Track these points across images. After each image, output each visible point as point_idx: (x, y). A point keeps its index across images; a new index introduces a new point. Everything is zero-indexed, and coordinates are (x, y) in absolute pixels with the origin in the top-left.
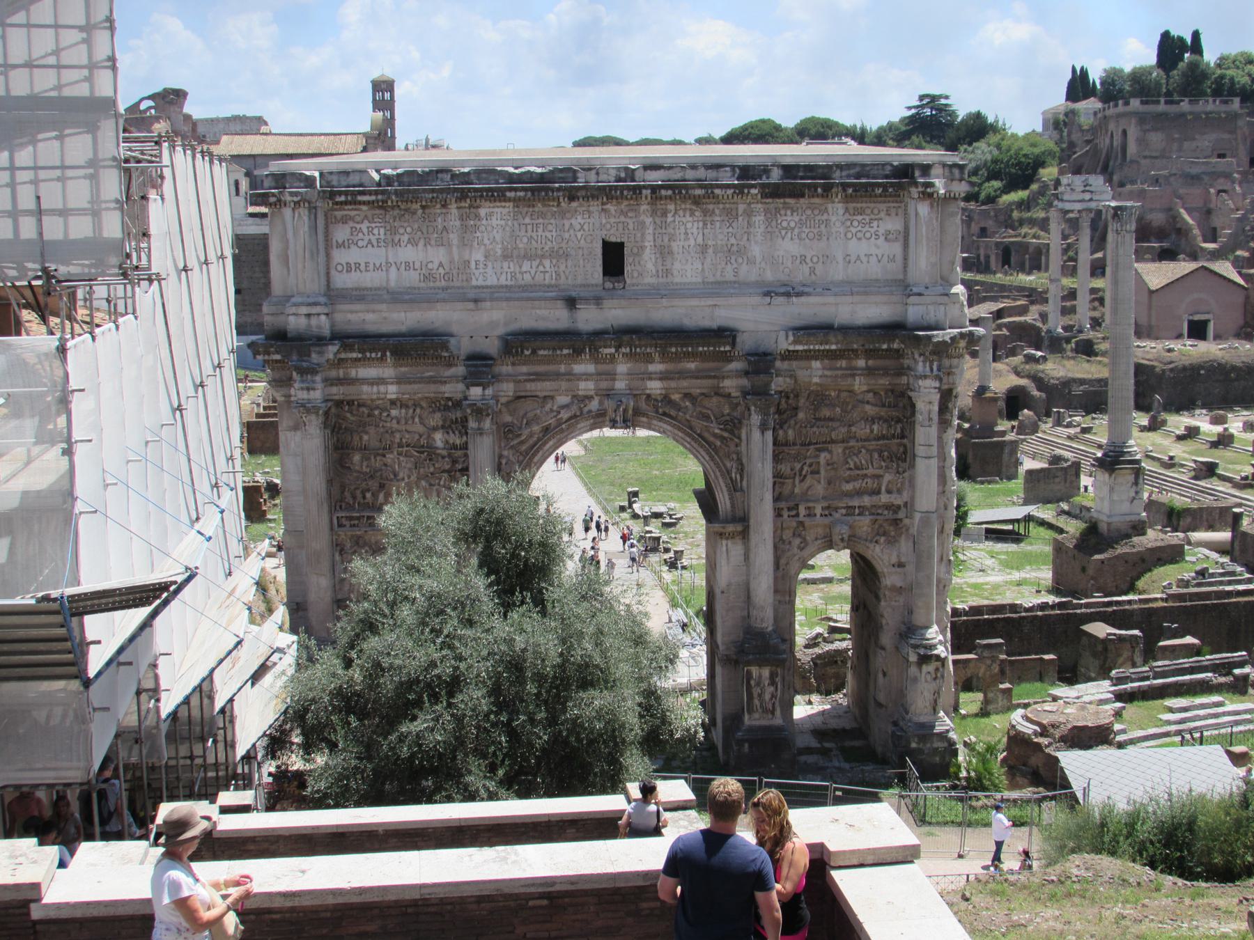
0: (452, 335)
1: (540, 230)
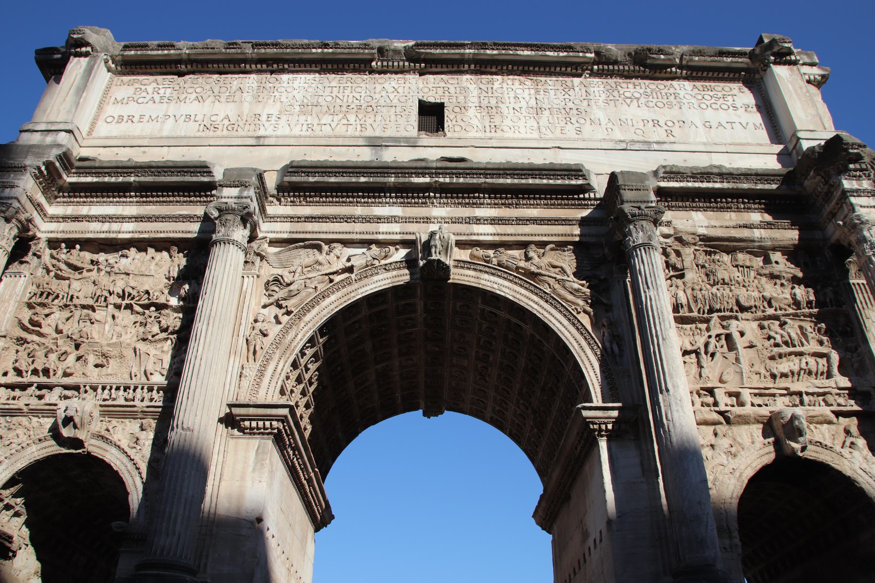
1: (347, 92)
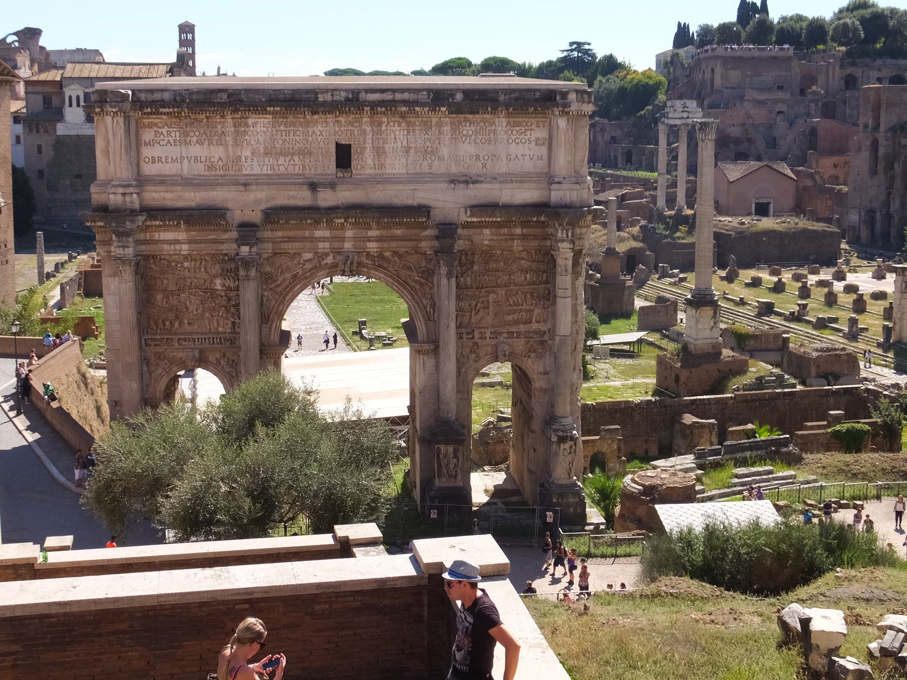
0: (229, 210)
1: (291, 135)
